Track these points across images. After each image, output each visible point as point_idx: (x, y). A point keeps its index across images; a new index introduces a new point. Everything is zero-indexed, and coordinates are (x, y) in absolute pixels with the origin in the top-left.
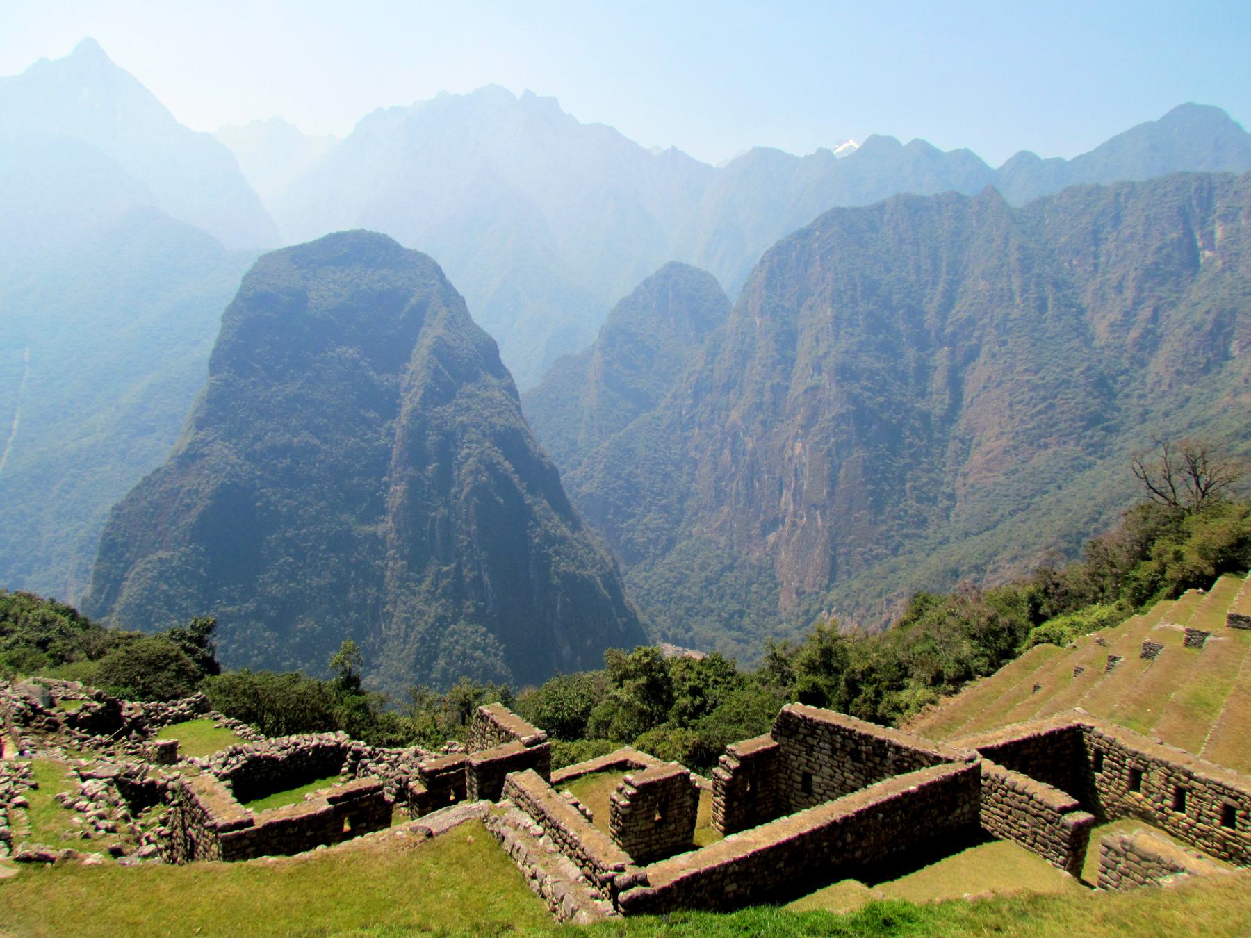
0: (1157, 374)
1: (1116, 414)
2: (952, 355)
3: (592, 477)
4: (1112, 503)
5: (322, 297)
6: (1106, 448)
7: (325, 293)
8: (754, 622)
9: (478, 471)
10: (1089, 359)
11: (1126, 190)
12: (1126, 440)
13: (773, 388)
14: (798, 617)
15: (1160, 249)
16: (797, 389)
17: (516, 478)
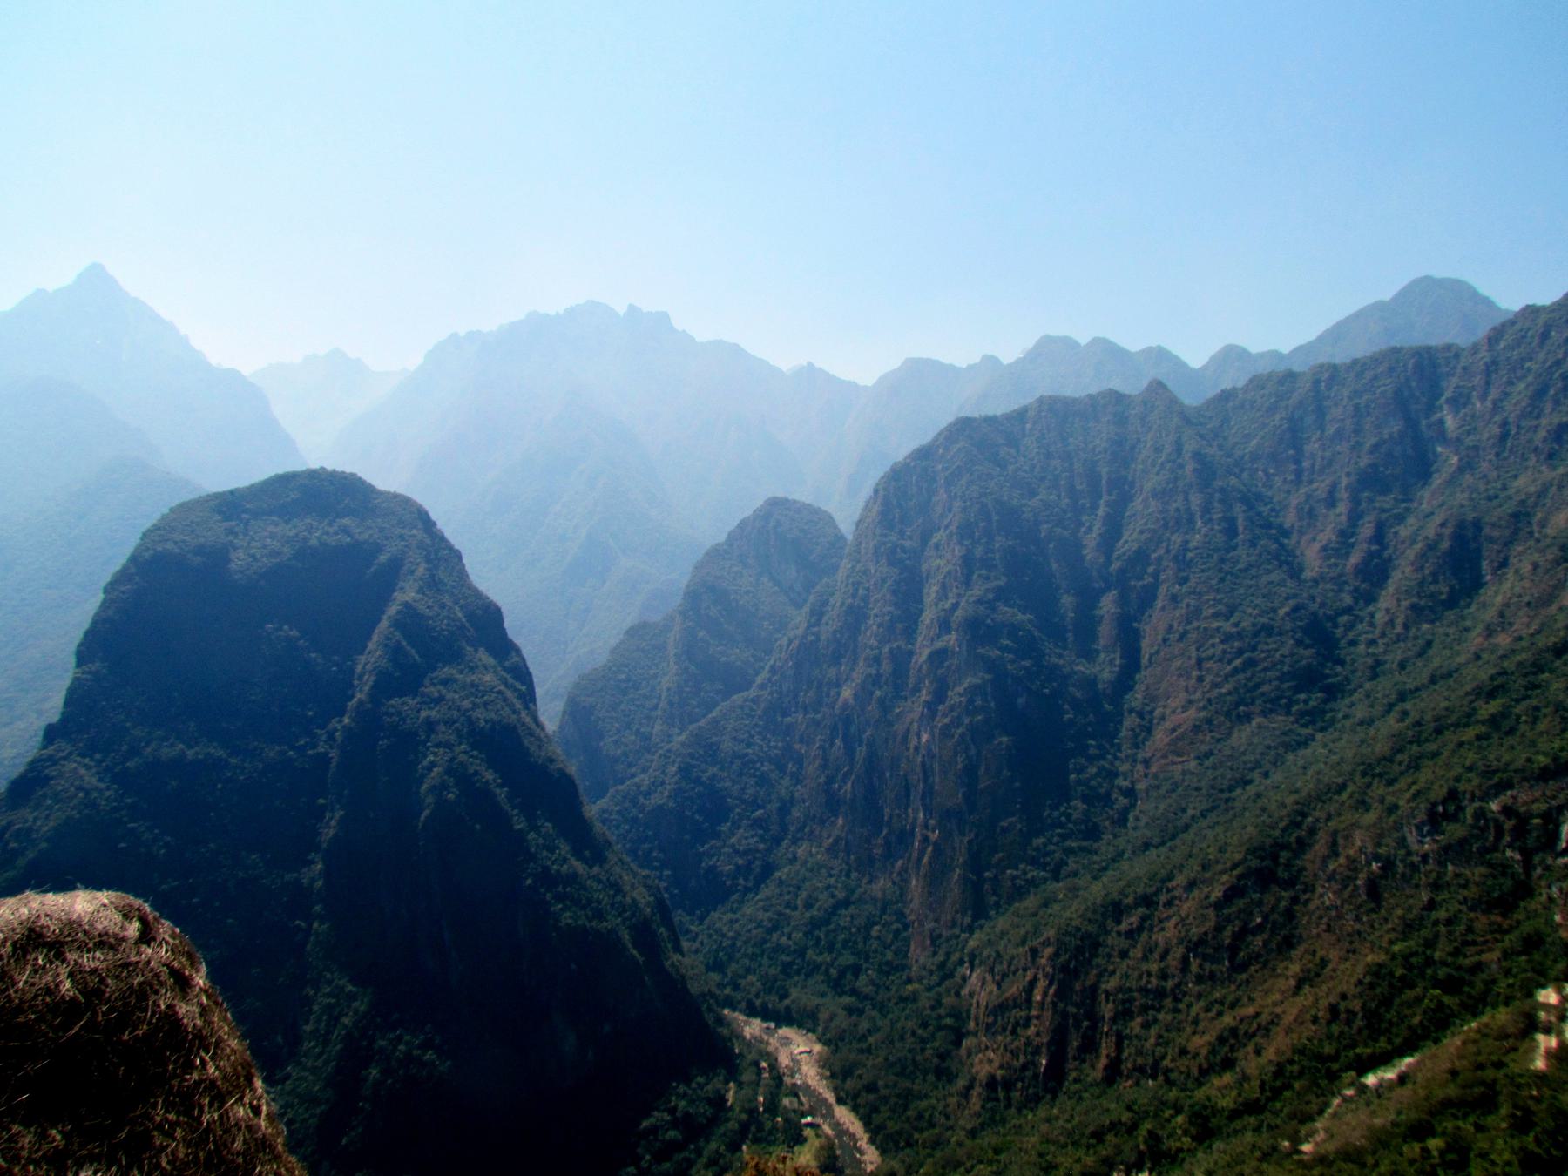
0: (1388, 610)
1: (1339, 669)
2: (1123, 600)
3: (663, 783)
4: (1319, 798)
5: (253, 556)
6: (1328, 716)
7: (256, 549)
8: (872, 982)
9: (443, 786)
10: (1295, 596)
11: (1326, 376)
12: (1352, 704)
13: (893, 655)
14: (931, 972)
15: (1376, 447)
16: (922, 655)
17: (502, 794)
